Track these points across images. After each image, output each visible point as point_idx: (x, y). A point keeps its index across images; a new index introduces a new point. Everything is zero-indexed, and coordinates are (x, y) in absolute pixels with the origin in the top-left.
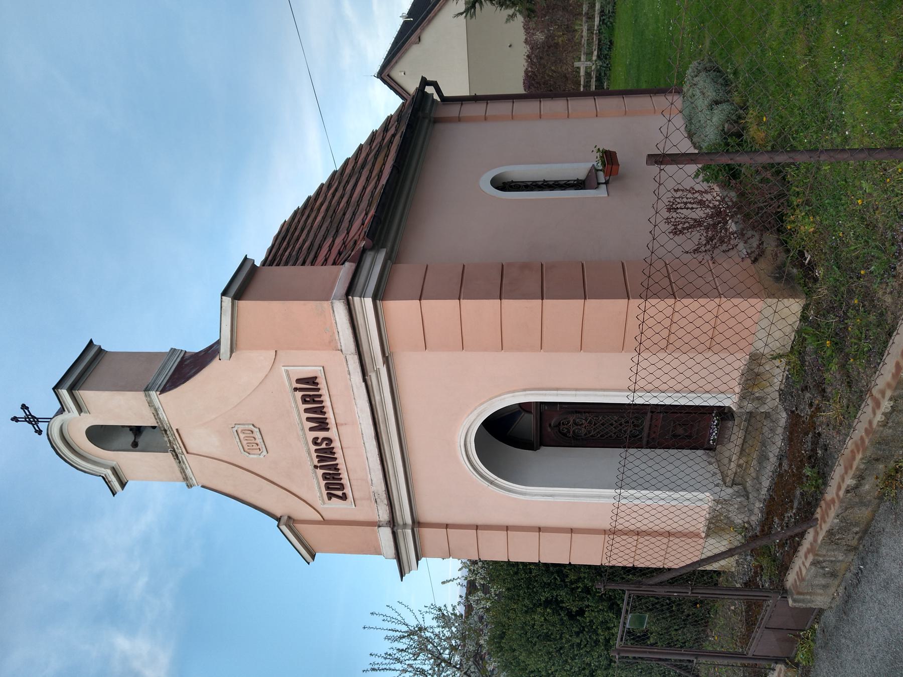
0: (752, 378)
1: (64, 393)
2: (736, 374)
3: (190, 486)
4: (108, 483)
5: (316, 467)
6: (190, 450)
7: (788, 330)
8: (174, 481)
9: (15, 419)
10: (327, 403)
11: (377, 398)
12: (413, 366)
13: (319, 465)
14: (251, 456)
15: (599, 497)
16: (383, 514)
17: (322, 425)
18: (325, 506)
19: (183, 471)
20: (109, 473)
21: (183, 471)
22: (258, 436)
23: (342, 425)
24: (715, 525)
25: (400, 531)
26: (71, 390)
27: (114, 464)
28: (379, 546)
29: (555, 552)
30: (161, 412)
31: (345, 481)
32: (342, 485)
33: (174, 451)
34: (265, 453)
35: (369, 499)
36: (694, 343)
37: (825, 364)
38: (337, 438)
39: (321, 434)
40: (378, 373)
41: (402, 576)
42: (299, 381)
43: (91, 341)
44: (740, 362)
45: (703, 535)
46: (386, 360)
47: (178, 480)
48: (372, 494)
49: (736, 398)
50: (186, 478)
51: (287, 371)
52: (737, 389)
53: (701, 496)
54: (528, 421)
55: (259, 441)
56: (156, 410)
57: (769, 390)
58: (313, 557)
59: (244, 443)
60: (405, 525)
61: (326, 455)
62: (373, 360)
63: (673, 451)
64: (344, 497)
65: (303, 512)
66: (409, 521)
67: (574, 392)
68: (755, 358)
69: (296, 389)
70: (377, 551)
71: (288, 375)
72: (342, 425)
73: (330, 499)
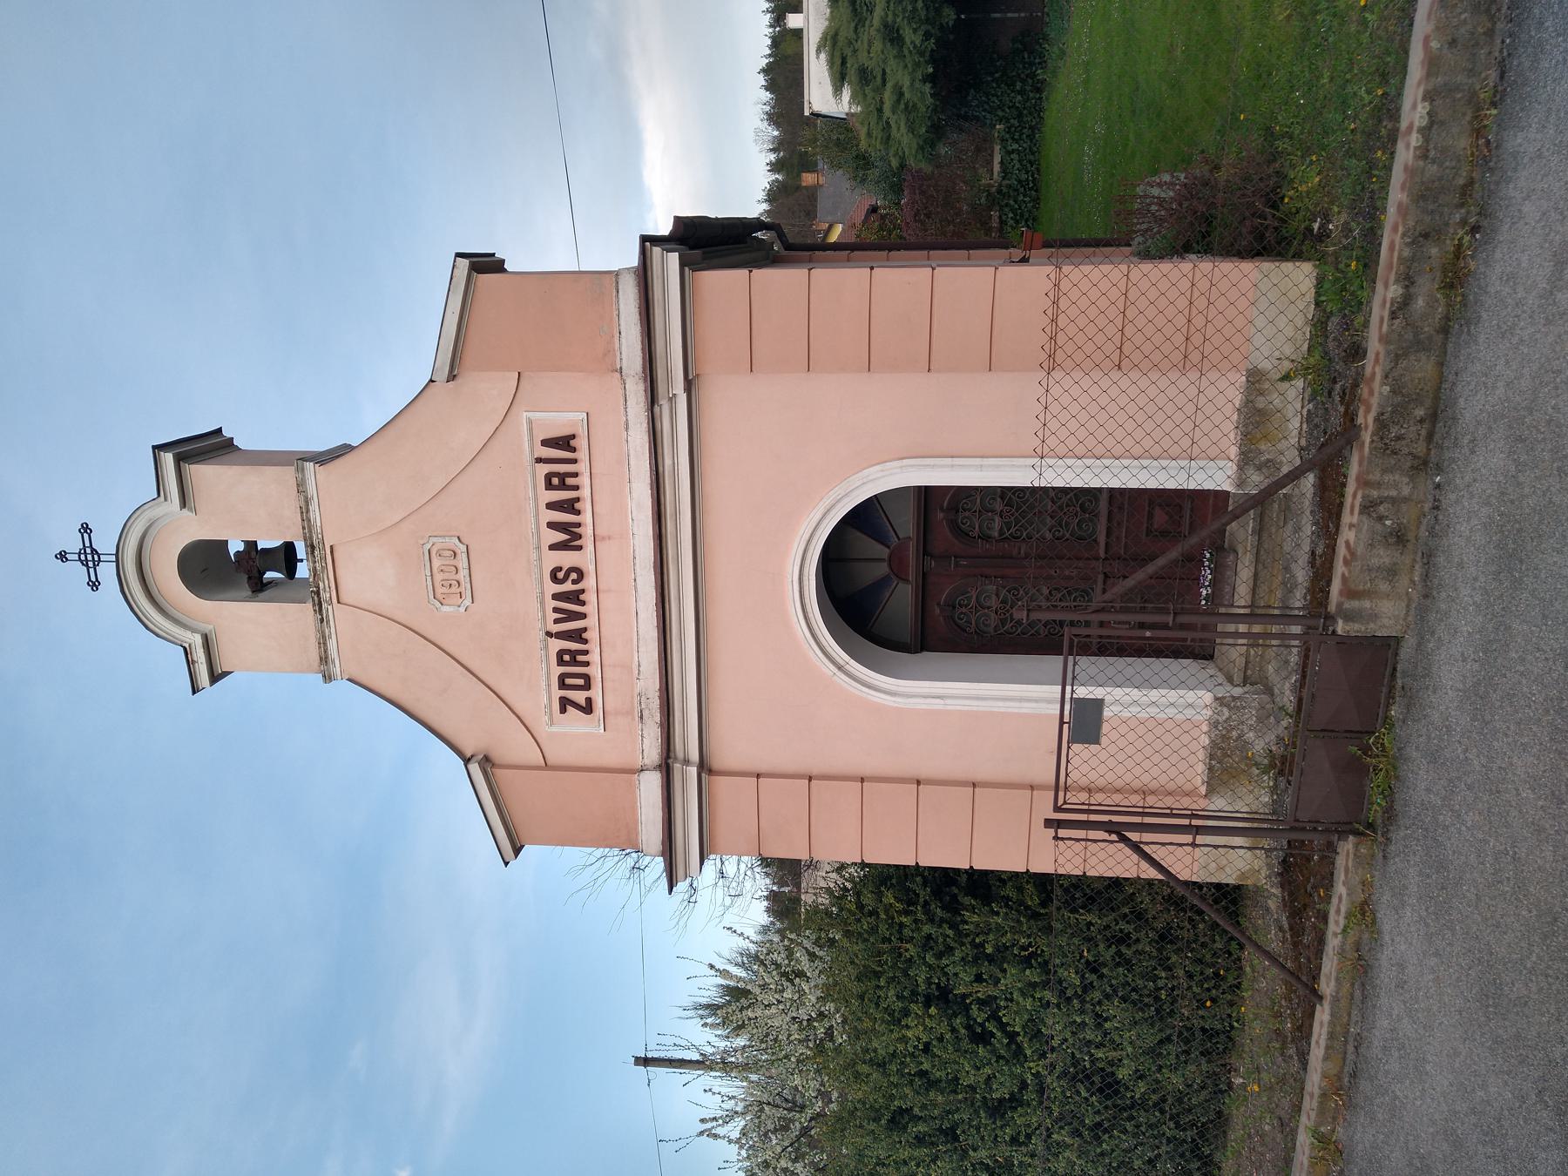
0: (1255, 421)
1: (168, 459)
2: (1229, 427)
3: (328, 678)
4: (190, 663)
5: (549, 634)
6: (343, 598)
7: (1300, 321)
8: (302, 671)
9: (62, 556)
10: (585, 493)
11: (668, 462)
12: (727, 397)
13: (556, 628)
14: (445, 609)
15: (1021, 700)
16: (652, 751)
17: (570, 538)
18: (554, 729)
19: (323, 642)
20: (197, 640)
21: (323, 642)
22: (462, 562)
23: (603, 538)
24: (1225, 763)
25: (677, 766)
26: (180, 459)
27: (208, 628)
28: (636, 822)
29: (945, 851)
30: (314, 506)
31: (594, 671)
32: (587, 678)
33: (318, 593)
34: (468, 602)
35: (630, 713)
36: (1157, 357)
37: (1360, 419)
38: (592, 568)
39: (567, 559)
40: (672, 399)
41: (670, 891)
42: (546, 443)
43: (220, 430)
44: (1229, 392)
45: (1203, 790)
46: (689, 385)
47: (309, 670)
48: (636, 700)
49: (1231, 468)
50: (324, 659)
51: (530, 422)
52: (1233, 451)
53: (1191, 696)
54: (905, 524)
55: (463, 573)
56: (307, 502)
57: (1283, 445)
58: (517, 851)
59: (438, 577)
60: (687, 762)
61: (570, 599)
62: (668, 372)
63: (1130, 660)
64: (588, 708)
65: (514, 747)
66: (694, 755)
67: (978, 461)
68: (1255, 378)
69: (539, 460)
70: (628, 842)
71: (531, 430)
72: (603, 538)
73: (563, 710)
